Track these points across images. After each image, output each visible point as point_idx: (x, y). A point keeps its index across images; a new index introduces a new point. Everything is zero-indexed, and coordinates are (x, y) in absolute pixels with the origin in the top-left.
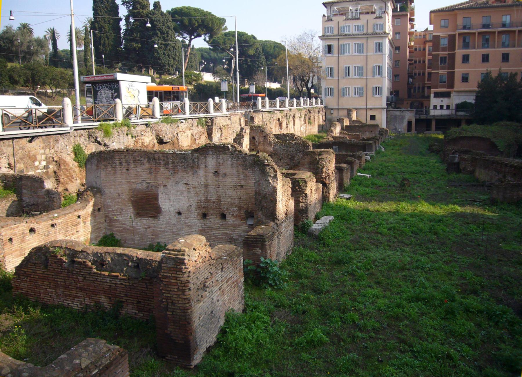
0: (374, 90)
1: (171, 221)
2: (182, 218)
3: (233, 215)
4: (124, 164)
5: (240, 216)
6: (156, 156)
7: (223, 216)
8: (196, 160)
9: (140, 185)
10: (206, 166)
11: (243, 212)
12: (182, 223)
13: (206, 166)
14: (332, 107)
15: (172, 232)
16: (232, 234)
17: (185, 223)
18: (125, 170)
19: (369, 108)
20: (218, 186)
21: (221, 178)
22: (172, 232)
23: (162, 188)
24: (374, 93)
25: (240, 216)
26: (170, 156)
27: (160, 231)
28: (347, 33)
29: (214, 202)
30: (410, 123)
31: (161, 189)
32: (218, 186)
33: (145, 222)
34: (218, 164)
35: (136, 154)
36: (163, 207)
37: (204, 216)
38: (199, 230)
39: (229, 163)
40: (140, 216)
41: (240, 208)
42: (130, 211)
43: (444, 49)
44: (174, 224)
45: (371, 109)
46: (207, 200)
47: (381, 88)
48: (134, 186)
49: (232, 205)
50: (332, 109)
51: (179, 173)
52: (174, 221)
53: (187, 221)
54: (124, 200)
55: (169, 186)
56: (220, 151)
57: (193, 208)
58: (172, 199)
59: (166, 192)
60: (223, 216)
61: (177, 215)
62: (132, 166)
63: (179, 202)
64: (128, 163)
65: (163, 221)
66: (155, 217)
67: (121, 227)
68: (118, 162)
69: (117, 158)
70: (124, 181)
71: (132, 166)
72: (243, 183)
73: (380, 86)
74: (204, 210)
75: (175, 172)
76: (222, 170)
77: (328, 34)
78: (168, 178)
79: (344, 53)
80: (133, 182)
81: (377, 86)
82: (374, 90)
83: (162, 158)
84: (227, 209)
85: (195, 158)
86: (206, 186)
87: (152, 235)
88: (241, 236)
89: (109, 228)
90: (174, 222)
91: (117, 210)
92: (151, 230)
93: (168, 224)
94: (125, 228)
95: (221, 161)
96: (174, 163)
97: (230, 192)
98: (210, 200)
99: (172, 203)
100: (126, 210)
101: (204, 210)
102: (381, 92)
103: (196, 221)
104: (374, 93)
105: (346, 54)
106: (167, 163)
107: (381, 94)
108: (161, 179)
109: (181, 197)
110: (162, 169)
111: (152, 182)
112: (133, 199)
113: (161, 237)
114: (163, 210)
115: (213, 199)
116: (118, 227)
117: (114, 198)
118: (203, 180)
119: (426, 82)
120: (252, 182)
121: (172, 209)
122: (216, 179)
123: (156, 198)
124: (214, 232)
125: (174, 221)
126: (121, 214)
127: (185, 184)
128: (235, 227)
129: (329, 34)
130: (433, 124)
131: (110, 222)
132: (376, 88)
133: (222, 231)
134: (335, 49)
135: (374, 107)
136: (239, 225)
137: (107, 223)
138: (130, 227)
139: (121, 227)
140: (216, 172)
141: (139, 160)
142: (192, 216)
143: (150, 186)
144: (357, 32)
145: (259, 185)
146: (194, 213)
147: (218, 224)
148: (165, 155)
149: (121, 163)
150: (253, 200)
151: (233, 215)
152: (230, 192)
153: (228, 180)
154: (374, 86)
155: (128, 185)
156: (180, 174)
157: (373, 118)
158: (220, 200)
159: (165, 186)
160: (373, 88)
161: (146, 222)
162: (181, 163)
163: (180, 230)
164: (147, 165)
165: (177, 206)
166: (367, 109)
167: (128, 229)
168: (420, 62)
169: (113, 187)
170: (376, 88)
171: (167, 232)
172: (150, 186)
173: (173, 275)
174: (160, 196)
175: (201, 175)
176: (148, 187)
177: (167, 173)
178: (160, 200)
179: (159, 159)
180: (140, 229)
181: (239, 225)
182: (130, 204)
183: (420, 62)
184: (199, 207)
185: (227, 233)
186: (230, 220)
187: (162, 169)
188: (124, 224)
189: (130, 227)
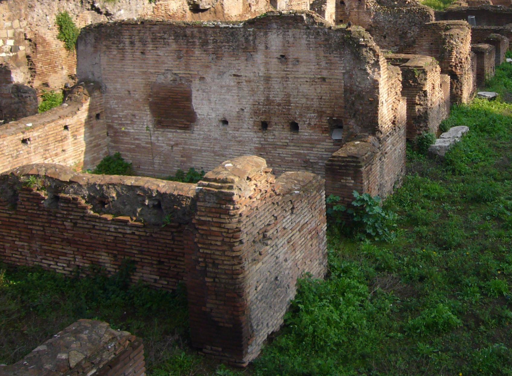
1: (212, 134)
2: (229, 129)
3: (309, 124)
4: (138, 44)
5: (320, 126)
6: (188, 32)
7: (294, 127)
9: (162, 77)
10: (267, 48)
11: (325, 120)
12: (229, 137)
13: (267, 48)
15: (214, 152)
16: (307, 155)
17: (235, 137)
18: (138, 54)
20: (286, 78)
21: (291, 66)
22: (214, 152)
23: (197, 81)
25: (320, 126)
26: (210, 32)
27: (195, 150)
29: (279, 105)
31: (196, 84)
32: (286, 78)
33: (170, 135)
34: (286, 44)
35: (156, 28)
36: (198, 111)
37: (264, 126)
38: (256, 148)
39: (304, 42)
40: (163, 127)
41: (321, 114)
44: (216, 139)
46: (268, 101)
48: (153, 79)
49: (308, 108)
51: (224, 59)
52: (216, 134)
53: (237, 134)
54: (137, 100)
55: (208, 80)
56: (288, 24)
57: (247, 114)
58: (213, 99)
59: (204, 88)
60: (294, 127)
61: (221, 124)
62: (150, 47)
63: (225, 104)
64: (144, 43)
65: (199, 134)
66: (186, 127)
67: (132, 144)
68: (127, 41)
69: (126, 34)
70: (137, 71)
71: (150, 47)
72: (325, 74)
74: (264, 117)
75: (218, 57)
76: (292, 54)
78: (208, 67)
80: (151, 73)
83: (197, 35)
84: (301, 116)
85: (250, 35)
86: (267, 79)
87: (182, 157)
88: (322, 158)
89: (113, 144)
90: (217, 136)
91: (126, 117)
92: (180, 148)
93: (207, 138)
94: (138, 146)
95: (291, 40)
96: (216, 42)
97: (305, 88)
98: (273, 101)
99: (213, 106)
100: (140, 117)
101: (264, 117)
106: (205, 43)
108: (195, 68)
109: (227, 97)
110: (197, 52)
111: (181, 72)
112: (151, 99)
113: (196, 160)
114: (198, 116)
115: (278, 100)
116: (127, 143)
118: (262, 69)
120: (339, 72)
121: (214, 115)
122: (283, 67)
123: (188, 97)
124: (280, 151)
125: (216, 134)
126: (133, 123)
127: (234, 75)
128: (312, 143)
131: (115, 136)
133: (293, 149)
136: (319, 141)
137: (111, 137)
138: (147, 143)
139: (132, 144)
141: (161, 38)
142: (245, 126)
143: (178, 79)
145: (351, 77)
146: (248, 122)
147: (286, 138)
148: (202, 30)
149: (132, 43)
150: (341, 101)
151: (309, 124)
152: (305, 88)
153: (302, 68)
155: (144, 77)
156: (226, 60)
158: (289, 102)
159: (202, 79)
161: (173, 135)
162: (228, 42)
163: (226, 148)
164: (174, 46)
165: (221, 111)
167: (144, 147)
169: (120, 80)
171: (205, 151)
172: (178, 79)
174: (194, 94)
175: (259, 61)
176: (174, 80)
177: (206, 58)
178: (194, 101)
179: (193, 36)
180: (162, 147)
181: (319, 141)
182: (147, 107)
184: (255, 113)
185: (300, 154)
186: (305, 133)
187: (197, 52)
188: (137, 139)
189: (147, 143)
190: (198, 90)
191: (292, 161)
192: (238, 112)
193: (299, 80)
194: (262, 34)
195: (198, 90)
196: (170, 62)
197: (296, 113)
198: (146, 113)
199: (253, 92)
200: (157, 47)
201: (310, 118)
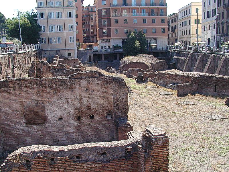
7: (92, 117)
8: (73, 83)
9: (30, 103)
10: (80, 86)
13: (80, 86)
14: (45, 50)
19: (67, 49)
21: (91, 92)
28: (52, 6)
29: (86, 108)
30: (90, 57)
31: (47, 104)
33: (35, 127)
34: (89, 84)
37: (79, 118)
39: (96, 82)
41: (103, 110)
42: (23, 121)
43: (104, 16)
45: (68, 50)
46: (81, 108)
50: (45, 51)
53: (67, 123)
57: (72, 114)
60: (92, 117)
62: (24, 90)
68: (12, 89)
69: (11, 86)
71: (24, 90)
72: (105, 94)
75: (57, 91)
77: (40, 6)
79: (51, 18)
81: (71, 37)
83: (48, 83)
84: (95, 112)
86: (81, 99)
87: (41, 136)
90: (58, 125)
91: (12, 122)
92: (40, 132)
94: (18, 134)
95: (91, 82)
96: (57, 85)
97: (97, 101)
99: (55, 112)
103: (74, 122)
105: (52, 19)
106: (51, 87)
110: (48, 91)
111: (40, 100)
117: (9, 114)
119: (91, 34)
120: (111, 93)
121: (56, 116)
125: (57, 123)
126: (15, 124)
128: (100, 122)
129: (41, 6)
130: (103, 56)
134: (45, 16)
136: (103, 121)
138: (23, 132)
140: (87, 89)
143: (38, 103)
144: (57, 6)
146: (72, 117)
147: (89, 121)
152: (97, 101)
156: (62, 92)
157: (70, 55)
158: (90, 106)
162: (62, 85)
164: (36, 89)
166: (66, 50)
167: (21, 134)
168: (86, 23)
172: (38, 103)
173: (161, 150)
174: (46, 108)
176: (37, 103)
177: (51, 93)
179: (45, 84)
180: (31, 133)
181: (103, 121)
183: (86, 23)
184: (75, 113)
186: (97, 118)
188: (18, 131)
189: (23, 132)
190: (48, 107)
191: (91, 130)
192: (67, 114)
193: (94, 98)
194: (78, 81)
195: (48, 107)
196: (34, 96)
197: (93, 111)
198: (22, 119)
199: (74, 105)
200: (27, 90)
201: (99, 112)
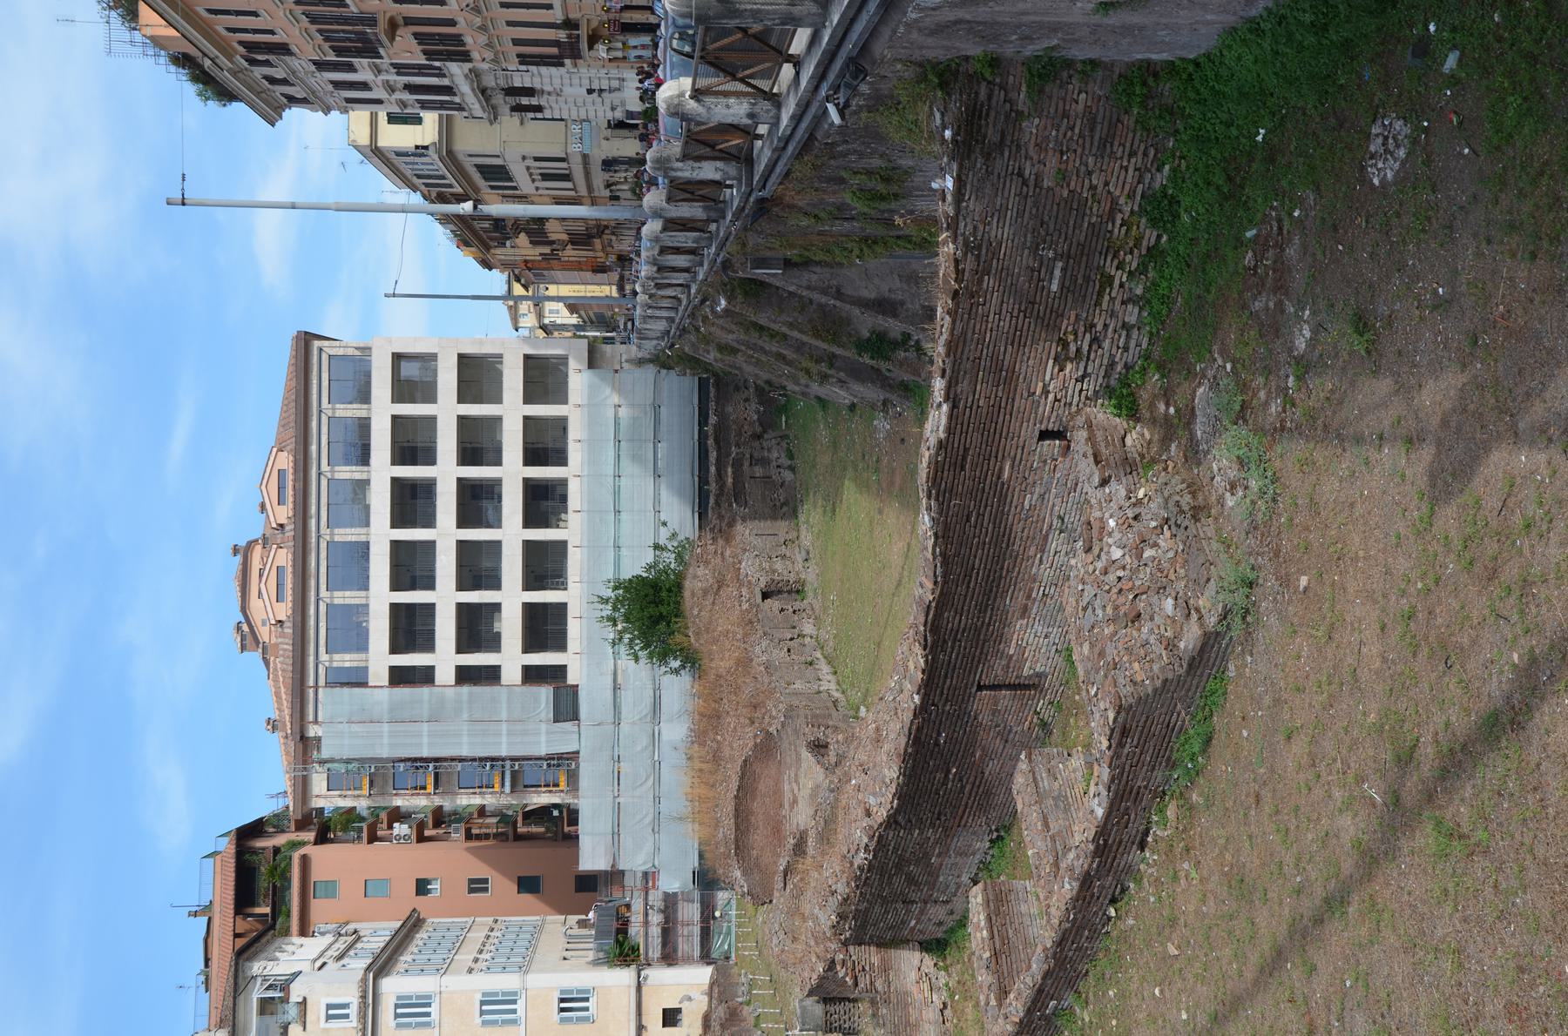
0: (569, 1020)
24: (579, 1019)
47: (562, 992)
73: (557, 995)
82: (569, 1020)
102: (579, 991)
104: (579, 1019)
107: (587, 991)
132: (563, 1010)
135: (633, 1016)
154: (556, 1016)
157: (671, 1017)
160: (563, 1020)
170: (563, 1010)
